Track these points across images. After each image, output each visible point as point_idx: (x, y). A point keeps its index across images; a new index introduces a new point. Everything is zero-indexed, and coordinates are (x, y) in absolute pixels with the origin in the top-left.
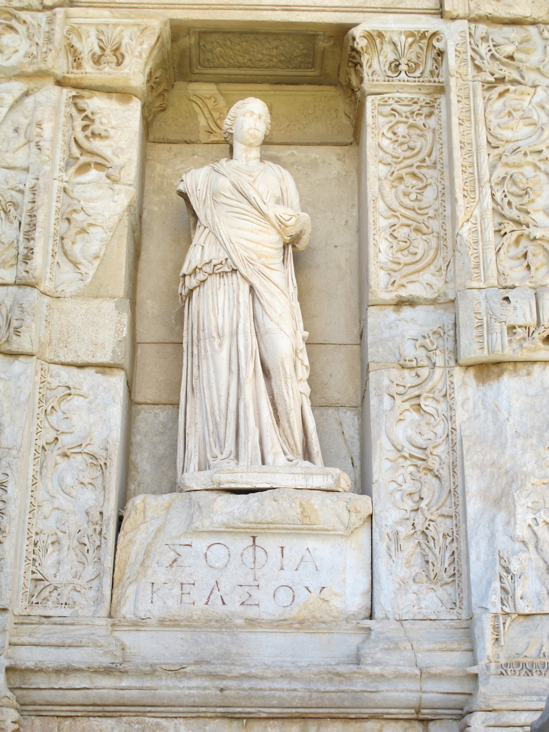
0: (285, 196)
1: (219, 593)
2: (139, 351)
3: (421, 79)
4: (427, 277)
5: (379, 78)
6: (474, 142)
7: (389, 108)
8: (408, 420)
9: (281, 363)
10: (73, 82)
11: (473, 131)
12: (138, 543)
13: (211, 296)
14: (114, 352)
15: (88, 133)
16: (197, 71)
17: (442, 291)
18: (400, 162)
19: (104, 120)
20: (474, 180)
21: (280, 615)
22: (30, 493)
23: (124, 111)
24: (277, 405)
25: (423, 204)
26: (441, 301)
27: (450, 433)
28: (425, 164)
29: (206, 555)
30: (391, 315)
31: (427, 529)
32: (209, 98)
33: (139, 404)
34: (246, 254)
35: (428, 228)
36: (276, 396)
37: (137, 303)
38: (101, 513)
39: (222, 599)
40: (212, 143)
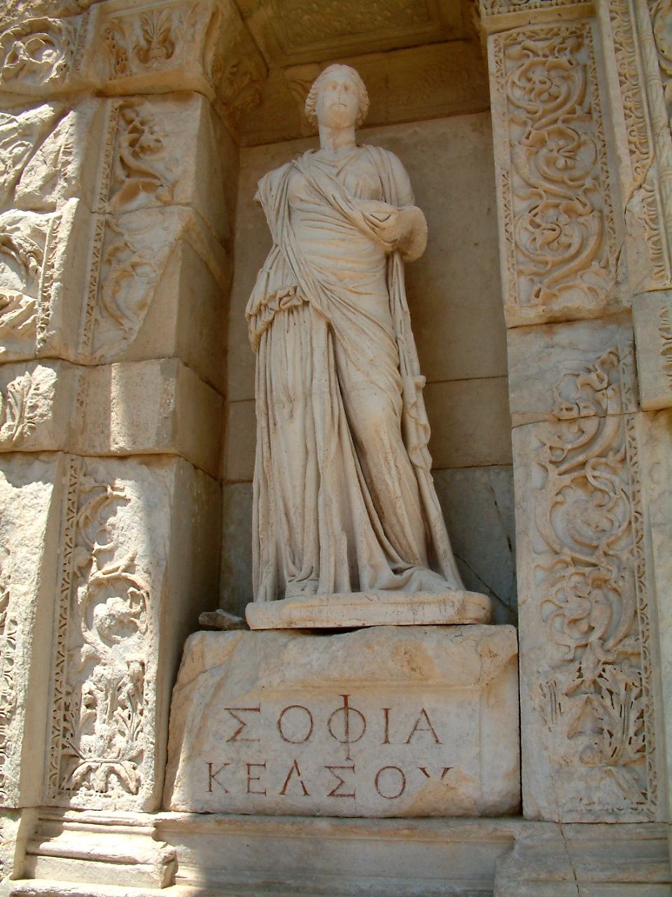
1: (300, 779)
4: (590, 278)
6: (640, 71)
7: (518, 48)
10: (119, 90)
11: (637, 58)
12: (195, 701)
14: (157, 434)
15: (137, 149)
18: (540, 119)
19: (156, 129)
20: (645, 126)
22: (57, 640)
23: (181, 112)
24: (378, 492)
25: (577, 173)
27: (633, 519)
29: (279, 723)
30: (536, 342)
31: (601, 676)
33: (233, 482)
35: (584, 205)
38: (143, 664)
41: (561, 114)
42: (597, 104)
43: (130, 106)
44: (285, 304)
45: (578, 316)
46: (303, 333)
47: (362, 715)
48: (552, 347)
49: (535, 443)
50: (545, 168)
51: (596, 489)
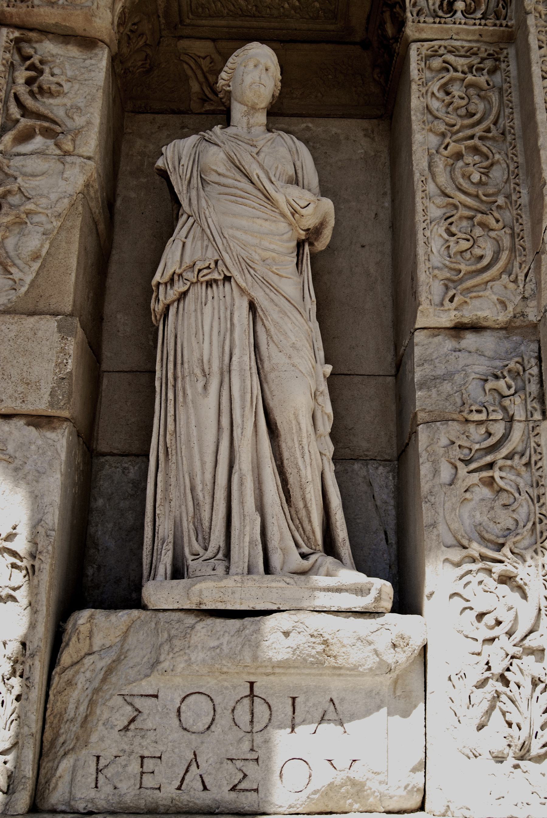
0: (300, 175)
1: (198, 772)
2: (105, 382)
3: (483, 22)
5: (427, 19)
7: (440, 60)
8: (477, 498)
9: (294, 414)
10: (16, 20)
12: (80, 686)
13: (193, 314)
16: (188, 21)
17: (519, 310)
19: (56, 71)
21: (290, 807)
23: (85, 60)
24: (288, 475)
26: (517, 324)
27: (537, 520)
28: (490, 135)
29: (179, 711)
32: (204, 58)
33: (104, 455)
34: (244, 254)
35: (498, 221)
36: (285, 462)
37: (105, 318)
39: (203, 782)
40: (207, 113)
41: (478, 130)
42: (511, 127)
43: (29, 41)
44: (204, 276)
45: (485, 324)
46: (222, 308)
47: (267, 703)
48: (460, 351)
49: (444, 441)
50: (461, 180)
51: (501, 490)
